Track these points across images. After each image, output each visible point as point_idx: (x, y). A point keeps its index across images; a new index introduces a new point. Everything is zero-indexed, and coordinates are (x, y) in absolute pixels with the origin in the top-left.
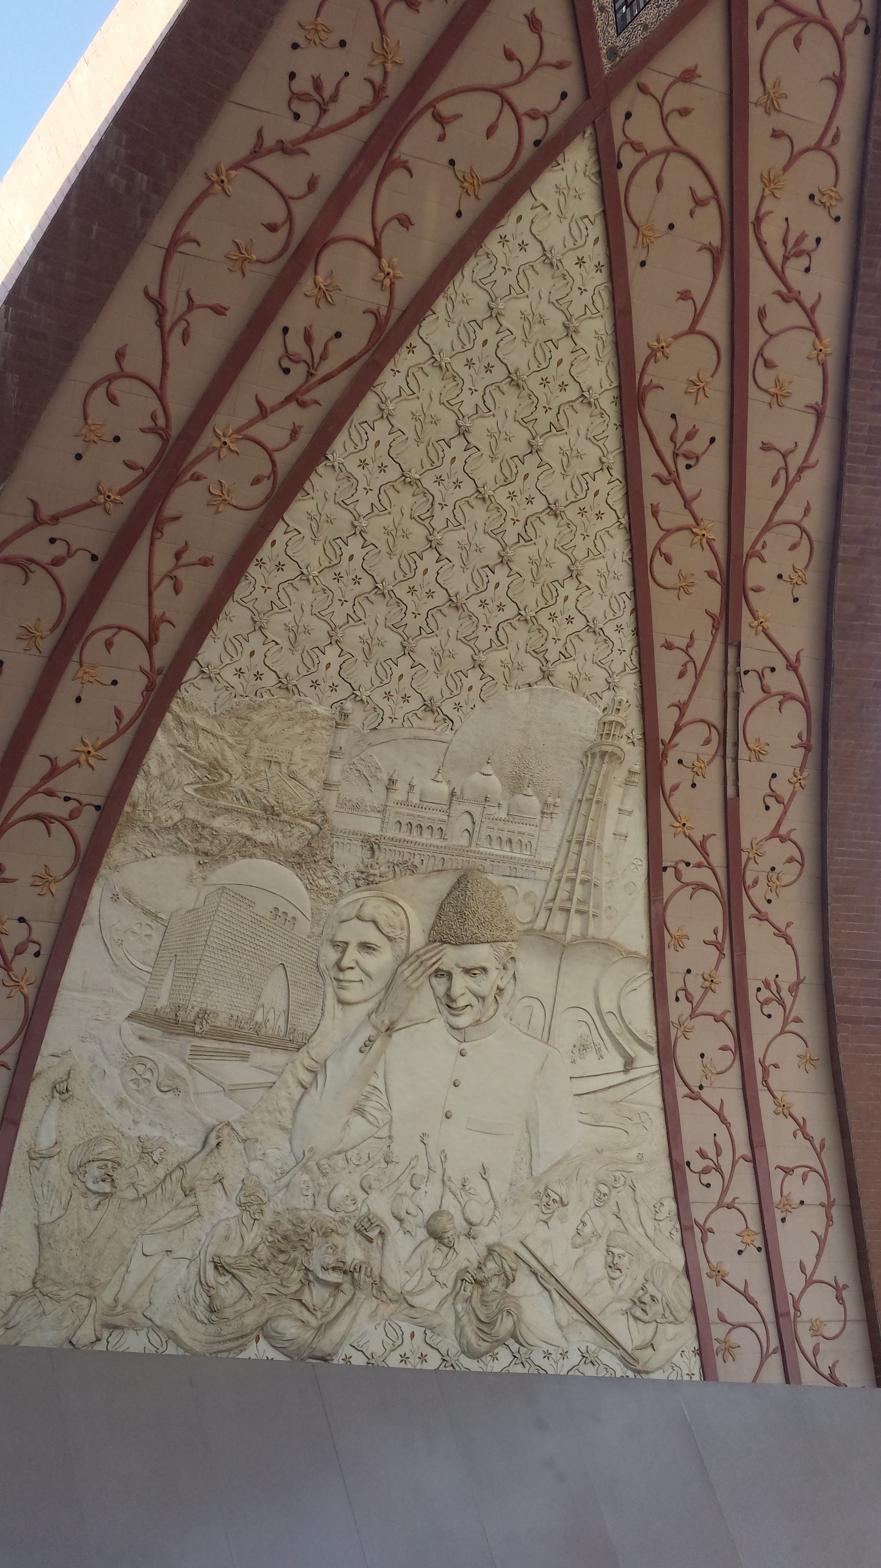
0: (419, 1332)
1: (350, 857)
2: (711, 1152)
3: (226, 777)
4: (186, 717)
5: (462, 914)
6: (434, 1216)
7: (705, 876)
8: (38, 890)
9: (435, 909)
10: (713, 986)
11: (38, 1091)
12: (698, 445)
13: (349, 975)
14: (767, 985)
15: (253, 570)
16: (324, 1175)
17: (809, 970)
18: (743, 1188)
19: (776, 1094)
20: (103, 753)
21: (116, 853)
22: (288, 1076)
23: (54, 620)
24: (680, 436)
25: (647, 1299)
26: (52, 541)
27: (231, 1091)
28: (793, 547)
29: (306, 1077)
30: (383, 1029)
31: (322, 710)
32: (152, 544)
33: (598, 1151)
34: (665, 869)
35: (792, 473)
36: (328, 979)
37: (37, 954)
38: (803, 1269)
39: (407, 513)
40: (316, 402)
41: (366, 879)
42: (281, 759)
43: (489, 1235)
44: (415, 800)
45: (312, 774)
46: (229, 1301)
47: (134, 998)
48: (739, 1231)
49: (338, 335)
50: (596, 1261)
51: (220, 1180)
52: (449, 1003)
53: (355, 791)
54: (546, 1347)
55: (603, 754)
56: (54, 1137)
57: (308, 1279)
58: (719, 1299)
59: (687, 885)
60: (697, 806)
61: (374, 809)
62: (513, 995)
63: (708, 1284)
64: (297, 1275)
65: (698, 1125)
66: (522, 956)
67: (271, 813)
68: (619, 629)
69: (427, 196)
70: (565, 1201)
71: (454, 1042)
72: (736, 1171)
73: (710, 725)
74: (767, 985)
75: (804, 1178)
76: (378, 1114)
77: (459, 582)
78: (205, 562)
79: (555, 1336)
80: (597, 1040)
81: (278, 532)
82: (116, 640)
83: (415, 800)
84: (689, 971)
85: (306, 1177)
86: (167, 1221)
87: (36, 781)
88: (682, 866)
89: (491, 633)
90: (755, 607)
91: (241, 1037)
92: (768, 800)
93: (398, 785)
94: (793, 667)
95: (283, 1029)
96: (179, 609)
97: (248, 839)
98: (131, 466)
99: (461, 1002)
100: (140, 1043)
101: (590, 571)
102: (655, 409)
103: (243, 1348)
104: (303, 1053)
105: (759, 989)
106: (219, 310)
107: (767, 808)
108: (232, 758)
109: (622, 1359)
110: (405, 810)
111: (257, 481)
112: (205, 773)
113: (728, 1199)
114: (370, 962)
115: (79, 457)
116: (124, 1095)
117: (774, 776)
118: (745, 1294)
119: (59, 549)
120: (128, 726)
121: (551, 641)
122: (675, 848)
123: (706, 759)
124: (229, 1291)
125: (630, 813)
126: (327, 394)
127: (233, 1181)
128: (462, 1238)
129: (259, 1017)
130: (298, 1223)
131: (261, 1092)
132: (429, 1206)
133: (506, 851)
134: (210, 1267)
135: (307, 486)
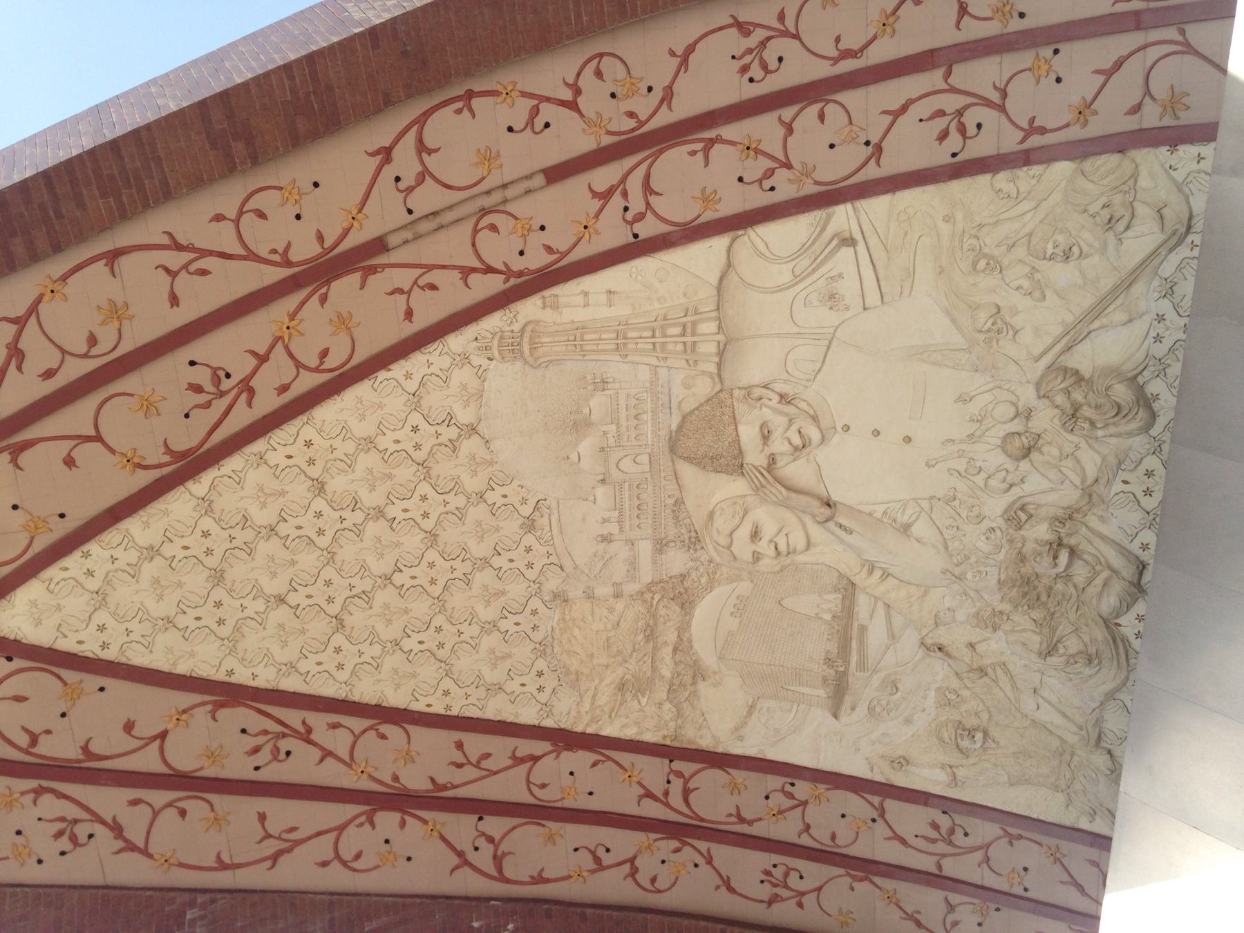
0: (1122, 475)
1: (676, 561)
2: (941, 123)
3: (628, 677)
4: (586, 719)
5: (712, 458)
6: (1010, 456)
7: (634, 185)
8: (742, 789)
9: (713, 476)
10: (753, 146)
11: (900, 780)
12: (202, 376)
13: (782, 547)
14: (745, 69)
16: (967, 558)
18: (980, 75)
19: (870, 37)
20: (626, 765)
21: (705, 743)
22: (878, 591)
24: (202, 398)
25: (1105, 214)
26: (476, 849)
27: (892, 636)
28: (261, 215)
30: (827, 512)
31: (556, 618)
32: (457, 787)
34: (636, 236)
35: (186, 256)
37: (793, 785)
40: (304, 723)
41: (694, 542)
42: (604, 638)
43: (1028, 395)
44: (616, 514)
46: (1081, 647)
47: (819, 716)
48: (1033, 81)
49: (244, 731)
50: (1062, 274)
51: (971, 646)
53: (619, 570)
54: (1150, 340)
56: (938, 770)
58: (1111, 117)
59: (648, 204)
60: (563, 215)
62: (785, 381)
63: (1096, 128)
64: (1059, 586)
65: (912, 146)
66: (744, 382)
67: (651, 634)
68: (408, 376)
69: (96, 721)
70: (995, 310)
71: (836, 438)
73: (476, 231)
74: (745, 69)
76: (909, 511)
77: (412, 541)
78: (460, 745)
79: (1140, 327)
80: (821, 283)
81: (419, 706)
82: (538, 783)
84: (740, 179)
85: (969, 576)
86: (1008, 690)
87: (658, 804)
90: (339, 231)
91: (846, 630)
93: (605, 533)
94: (386, 154)
95: (836, 596)
96: (500, 747)
97: (675, 650)
101: (362, 429)
102: (187, 437)
103: (1125, 640)
104: (857, 580)
105: (751, 80)
106: (262, 817)
107: (547, 125)
108: (612, 677)
109: (1171, 250)
110: (627, 523)
111: (383, 737)
113: (995, 97)
114: (769, 530)
115: (409, 859)
117: (510, 129)
118: (1109, 73)
119: (481, 842)
120: (602, 754)
121: (441, 439)
122: (612, 234)
124: (1073, 645)
125: (586, 294)
126: (294, 717)
127: (974, 635)
128: (1030, 425)
129: (828, 617)
131: (893, 613)
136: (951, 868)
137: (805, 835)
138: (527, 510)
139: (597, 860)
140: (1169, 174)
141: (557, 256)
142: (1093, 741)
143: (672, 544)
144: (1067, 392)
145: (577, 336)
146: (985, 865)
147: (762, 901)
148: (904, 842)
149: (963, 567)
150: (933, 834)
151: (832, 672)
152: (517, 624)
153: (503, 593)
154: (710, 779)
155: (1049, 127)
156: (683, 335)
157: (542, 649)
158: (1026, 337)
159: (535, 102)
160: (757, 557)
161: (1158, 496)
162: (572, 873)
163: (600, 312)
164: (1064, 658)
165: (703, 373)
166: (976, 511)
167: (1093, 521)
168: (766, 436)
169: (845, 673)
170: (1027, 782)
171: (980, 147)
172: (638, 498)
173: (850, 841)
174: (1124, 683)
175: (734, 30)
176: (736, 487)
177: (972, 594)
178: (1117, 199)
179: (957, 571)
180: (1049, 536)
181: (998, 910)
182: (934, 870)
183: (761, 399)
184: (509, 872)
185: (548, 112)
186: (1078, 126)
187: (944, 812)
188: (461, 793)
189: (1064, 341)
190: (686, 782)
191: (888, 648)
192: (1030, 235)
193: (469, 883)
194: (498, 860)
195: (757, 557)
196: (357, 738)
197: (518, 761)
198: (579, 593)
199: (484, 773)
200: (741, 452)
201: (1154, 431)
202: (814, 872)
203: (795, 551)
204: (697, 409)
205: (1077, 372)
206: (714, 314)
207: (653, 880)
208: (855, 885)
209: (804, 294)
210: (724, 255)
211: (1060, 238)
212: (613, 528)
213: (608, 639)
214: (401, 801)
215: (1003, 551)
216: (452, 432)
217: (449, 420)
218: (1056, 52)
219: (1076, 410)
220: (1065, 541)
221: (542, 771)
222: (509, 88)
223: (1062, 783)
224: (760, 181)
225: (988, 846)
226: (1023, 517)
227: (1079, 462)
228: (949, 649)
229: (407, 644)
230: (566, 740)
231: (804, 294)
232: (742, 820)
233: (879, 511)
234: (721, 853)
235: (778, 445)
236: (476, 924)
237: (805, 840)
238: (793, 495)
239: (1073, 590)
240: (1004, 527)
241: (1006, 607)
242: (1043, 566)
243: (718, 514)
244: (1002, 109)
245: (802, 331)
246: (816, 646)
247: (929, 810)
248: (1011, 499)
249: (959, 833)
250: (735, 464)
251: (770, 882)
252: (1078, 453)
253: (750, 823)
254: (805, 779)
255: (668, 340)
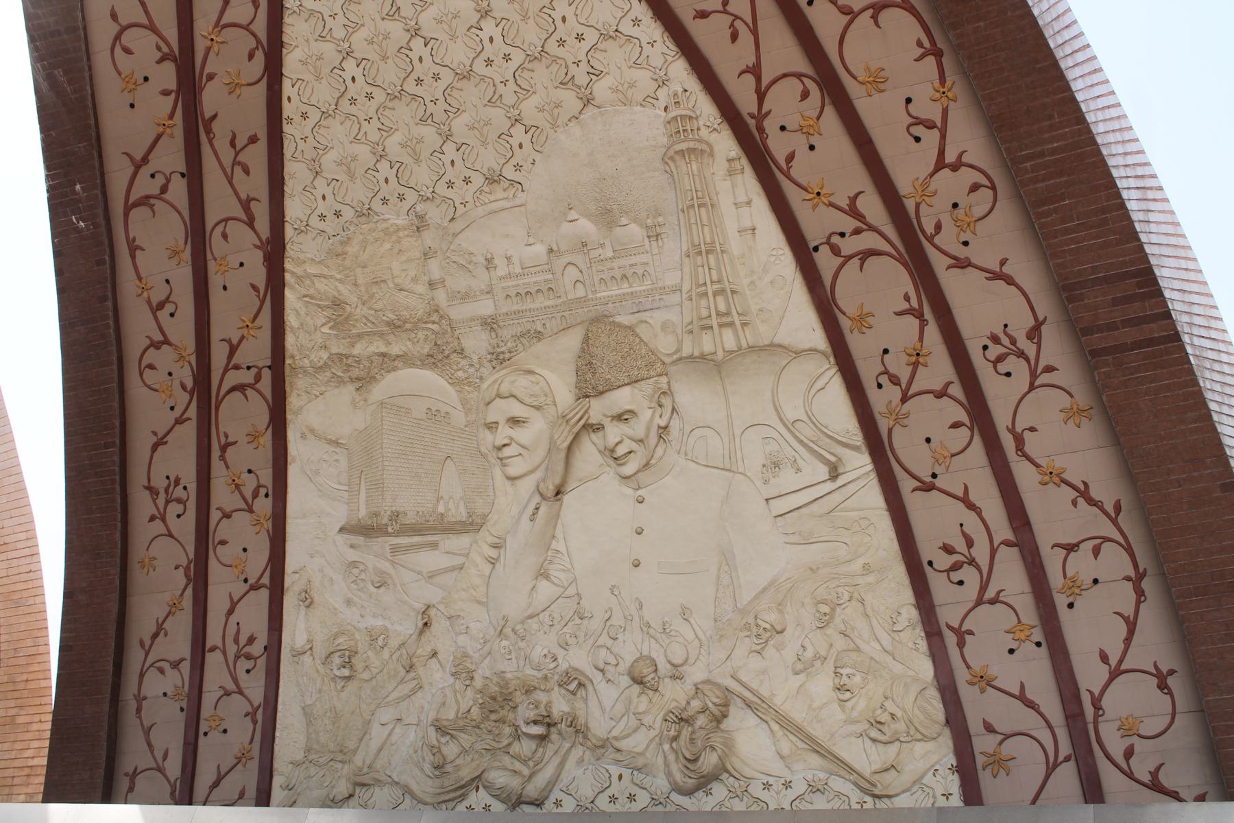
0: (626, 773)
1: (477, 343)
2: (960, 545)
5: (590, 363)
6: (632, 666)
8: (254, 445)
9: (573, 367)
10: (921, 360)
13: (507, 452)
14: (995, 339)
15: (287, 128)
17: (1046, 306)
18: (1011, 576)
19: (1038, 461)
20: (258, 322)
21: (294, 401)
22: (474, 556)
23: (183, 235)
25: (884, 717)
26: (153, 176)
27: (432, 576)
29: (493, 553)
30: (550, 492)
31: (401, 221)
32: (212, 145)
33: (811, 569)
34: (816, 249)
36: (493, 461)
37: (267, 495)
38: (1104, 658)
39: (378, 18)
41: (499, 359)
42: (385, 277)
43: (696, 674)
44: (518, 270)
45: (415, 280)
47: (340, 515)
48: (1008, 627)
50: (822, 685)
51: (435, 654)
52: (612, 455)
53: (460, 282)
54: (765, 779)
55: (681, 153)
56: (305, 637)
57: (517, 735)
59: (850, 257)
61: (482, 292)
62: (682, 430)
63: (967, 694)
64: (507, 730)
65: (935, 520)
66: (675, 387)
67: (395, 326)
68: (636, 22)
70: (779, 628)
71: (629, 491)
72: (996, 561)
73: (799, 76)
74: (995, 339)
75: (1096, 551)
76: (562, 576)
77: (459, 54)
78: (253, 140)
79: (777, 768)
80: (789, 452)
81: (287, 89)
82: (228, 230)
83: (518, 270)
84: (886, 351)
85: (505, 643)
87: (225, 361)
88: (836, 239)
89: (511, 86)
91: (431, 528)
92: (912, 130)
93: (496, 261)
95: (464, 514)
96: (256, 184)
97: (384, 355)
98: (166, 93)
99: (621, 451)
100: (352, 550)
103: (463, 797)
105: (985, 348)
107: (918, 139)
108: (346, 292)
109: (856, 784)
111: (251, 56)
112: (331, 311)
113: (990, 594)
115: (132, 106)
116: (350, 595)
117: (909, 101)
118: (1022, 698)
119: (159, 180)
121: (573, 68)
122: (817, 223)
123: (815, 114)
124: (451, 750)
125: (749, 203)
127: (446, 654)
128: (667, 680)
129: (441, 509)
130: (504, 684)
131: (455, 573)
132: (629, 657)
133: (625, 288)
134: (432, 731)
135: (285, 39)
136: (214, 661)
137: (220, 515)
138: (509, 172)
139: (161, 305)
140: (929, 769)
141: (785, 167)
142: (359, 779)
143: (493, 335)
144: (704, 710)
145: (701, 203)
146: (222, 692)
147: (149, 480)
148: (230, 612)
149: (512, 635)
150: (243, 640)
151: (385, 521)
152: (387, 181)
153: (417, 161)
154: (259, 412)
155: (965, 649)
156: (718, 314)
157: (364, 213)
158: (755, 663)
159: (939, 125)
160: (492, 426)
161: (610, 808)
162: (144, 281)
163: (731, 219)
164: (436, 743)
165: (680, 343)
166: (572, 641)
167: (578, 752)
168: (620, 417)
169: (387, 534)
170: (309, 724)
171: (939, 586)
172: (538, 291)
173: (221, 559)
174: (420, 801)
175: (1032, 323)
176: (563, 392)
177: (488, 645)
178: (901, 726)
179: (508, 630)
180: (556, 714)
181: (182, 710)
182: (209, 645)
183: (660, 406)
184: (135, 214)
185: (931, 138)
186: (969, 677)
187: (265, 648)
188: (206, 149)
189: (755, 699)
190: (251, 386)
191: (419, 573)
192: (858, 649)
193: (118, 174)
194: (145, 201)
195: (492, 426)
196: (246, 28)
197: (246, 205)
198: (429, 242)
199: (229, 170)
200: (602, 393)
201: (675, 797)
202: (186, 527)
203: (504, 465)
204: (641, 340)
205: (725, 716)
206: (744, 345)
207: (151, 367)
208: (181, 570)
209: (775, 435)
210: (807, 346)
211: (857, 679)
212: (502, 270)
213: (384, 281)
214: (189, 85)
215: (535, 673)
216: (582, 80)
217: (595, 74)
218: (1038, 644)
219: (686, 721)
220: (553, 729)
221: (238, 231)
222: (949, 94)
223: (313, 756)
224: (886, 372)
225: (240, 692)
226: (573, 686)
227: (635, 731)
228: (427, 633)
229: (350, 65)
230: (274, 253)
231: (775, 435)
232: (224, 449)
233: (558, 545)
234: (189, 432)
235: (614, 432)
236: (78, 187)
237: (215, 516)
238: (562, 455)
239: (505, 743)
240: (559, 670)
241: (478, 683)
242: (525, 712)
243: (532, 378)
244: (979, 602)
245: (737, 440)
246: (409, 501)
247: (266, 634)
248: (589, 673)
249: (249, 664)
250: (587, 390)
251: (169, 485)
252: (643, 729)
253: (222, 458)
254: (274, 507)
255: (711, 298)
